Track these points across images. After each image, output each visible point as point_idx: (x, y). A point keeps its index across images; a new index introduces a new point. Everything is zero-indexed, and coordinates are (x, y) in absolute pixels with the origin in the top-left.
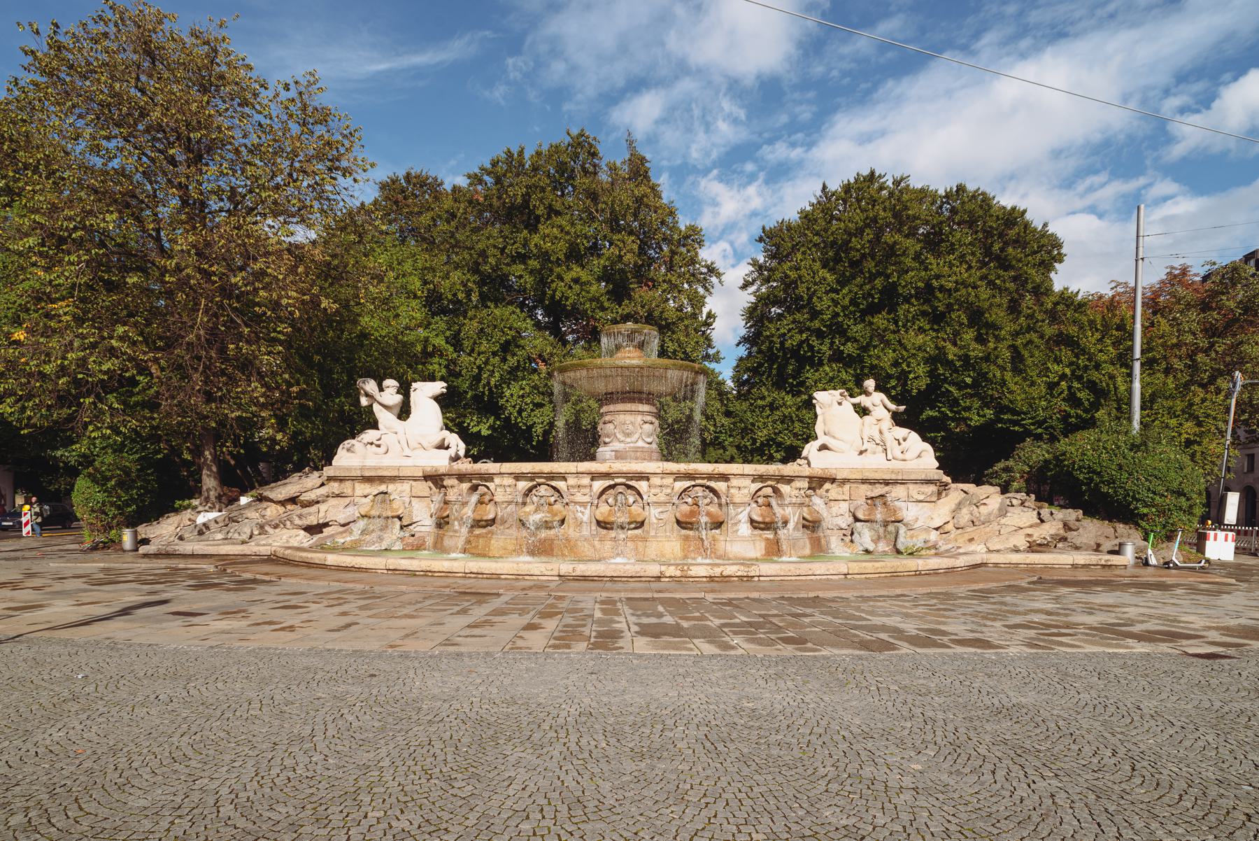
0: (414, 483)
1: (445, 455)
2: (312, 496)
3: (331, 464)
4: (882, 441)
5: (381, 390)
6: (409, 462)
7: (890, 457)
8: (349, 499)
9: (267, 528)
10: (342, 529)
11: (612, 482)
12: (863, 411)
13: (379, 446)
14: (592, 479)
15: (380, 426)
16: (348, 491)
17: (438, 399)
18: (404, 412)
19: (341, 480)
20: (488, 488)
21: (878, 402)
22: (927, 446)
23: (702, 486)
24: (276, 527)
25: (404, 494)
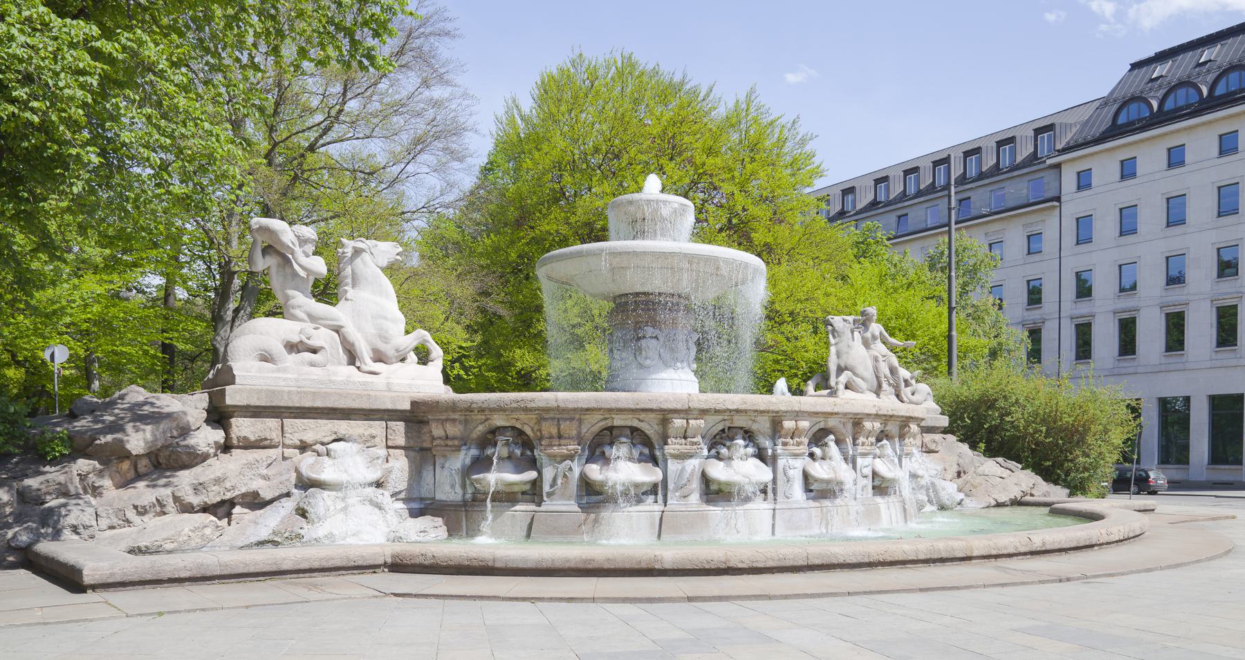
13: (314, 351)
16: (275, 436)
17: (391, 270)
21: (877, 333)
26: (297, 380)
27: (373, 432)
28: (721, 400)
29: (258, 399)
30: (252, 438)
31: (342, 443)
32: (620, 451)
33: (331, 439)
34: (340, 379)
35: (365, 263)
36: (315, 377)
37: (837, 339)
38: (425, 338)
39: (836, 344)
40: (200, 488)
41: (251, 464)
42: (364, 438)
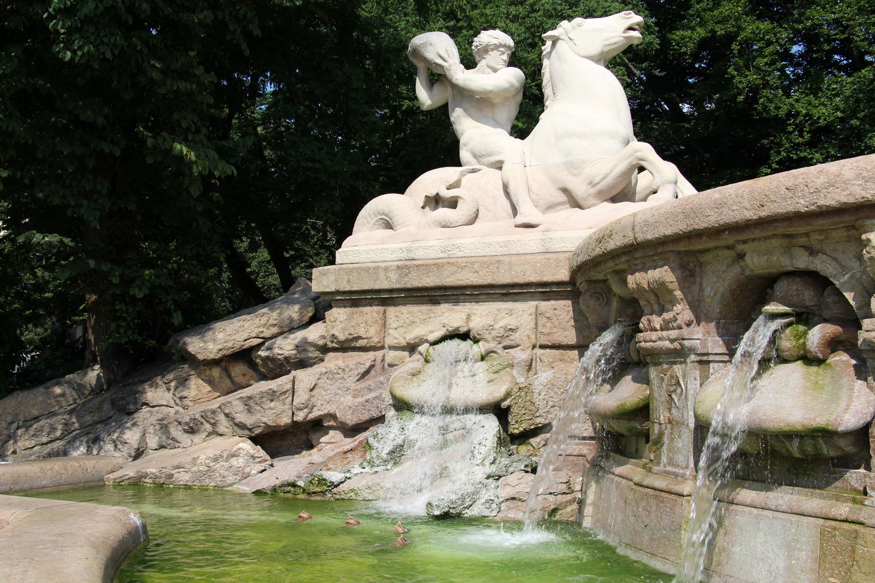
0: (545, 306)
2: (285, 347)
3: (332, 262)
6: (530, 241)
8: (367, 358)
9: (176, 432)
10: (349, 443)
13: (453, 203)
15: (464, 154)
24: (192, 431)
25: (516, 337)
27: (511, 322)
29: (348, 281)
30: (342, 337)
31: (456, 342)
36: (435, 243)
38: (639, 154)
40: (251, 403)
41: (331, 372)
42: (494, 333)
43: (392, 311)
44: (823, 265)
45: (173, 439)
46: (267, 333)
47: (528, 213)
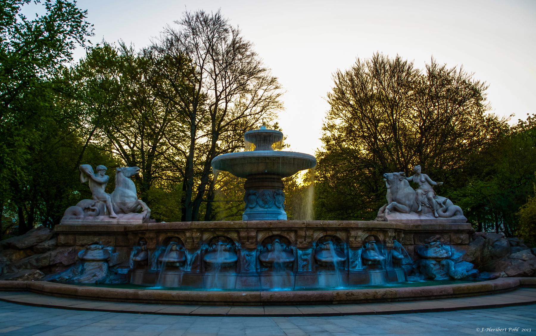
1: (141, 216)
4: (430, 205)
5: (96, 172)
6: (114, 221)
7: (437, 215)
8: (71, 249)
11: (271, 234)
12: (415, 186)
13: (93, 210)
14: (257, 233)
18: (111, 188)
19: (66, 234)
20: (179, 239)
21: (423, 179)
22: (458, 207)
23: (330, 236)
26: (82, 222)
27: (110, 240)
28: (205, 224)
32: (220, 246)
33: (91, 243)
34: (99, 220)
35: (121, 176)
36: (89, 220)
37: (391, 185)
39: (390, 188)
43: (77, 237)
44: (180, 237)
45: (13, 271)
46: (39, 241)
47: (114, 214)
